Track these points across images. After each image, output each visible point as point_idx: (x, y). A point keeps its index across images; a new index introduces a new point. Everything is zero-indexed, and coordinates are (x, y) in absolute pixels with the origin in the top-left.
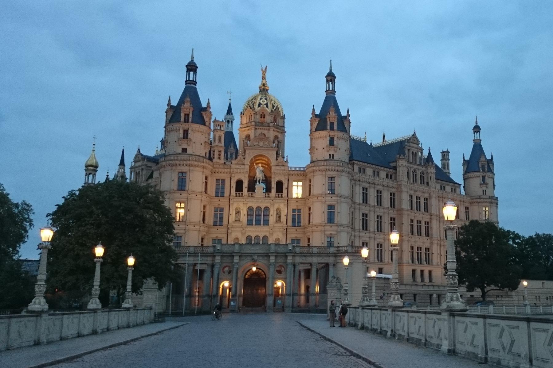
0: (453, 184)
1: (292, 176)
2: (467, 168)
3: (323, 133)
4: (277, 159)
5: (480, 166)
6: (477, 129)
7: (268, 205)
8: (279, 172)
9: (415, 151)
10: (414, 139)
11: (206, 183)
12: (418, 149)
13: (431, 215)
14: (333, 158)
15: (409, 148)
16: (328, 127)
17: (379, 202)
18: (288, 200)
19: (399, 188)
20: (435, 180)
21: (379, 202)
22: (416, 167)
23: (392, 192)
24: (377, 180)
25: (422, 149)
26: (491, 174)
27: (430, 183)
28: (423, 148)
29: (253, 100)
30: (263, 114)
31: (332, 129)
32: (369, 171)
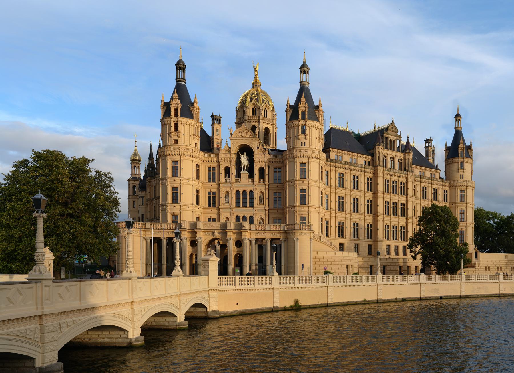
0: (431, 169)
1: (272, 164)
2: (448, 154)
3: (295, 123)
4: (258, 148)
9: (392, 138)
10: (392, 128)
11: (198, 171)
12: (396, 136)
13: (407, 198)
14: (305, 145)
15: (387, 135)
17: (356, 186)
21: (356, 186)
23: (368, 177)
25: (400, 137)
26: (469, 160)
27: (407, 168)
28: (402, 136)
29: (246, 96)
30: (254, 108)
31: (303, 118)
32: (347, 157)
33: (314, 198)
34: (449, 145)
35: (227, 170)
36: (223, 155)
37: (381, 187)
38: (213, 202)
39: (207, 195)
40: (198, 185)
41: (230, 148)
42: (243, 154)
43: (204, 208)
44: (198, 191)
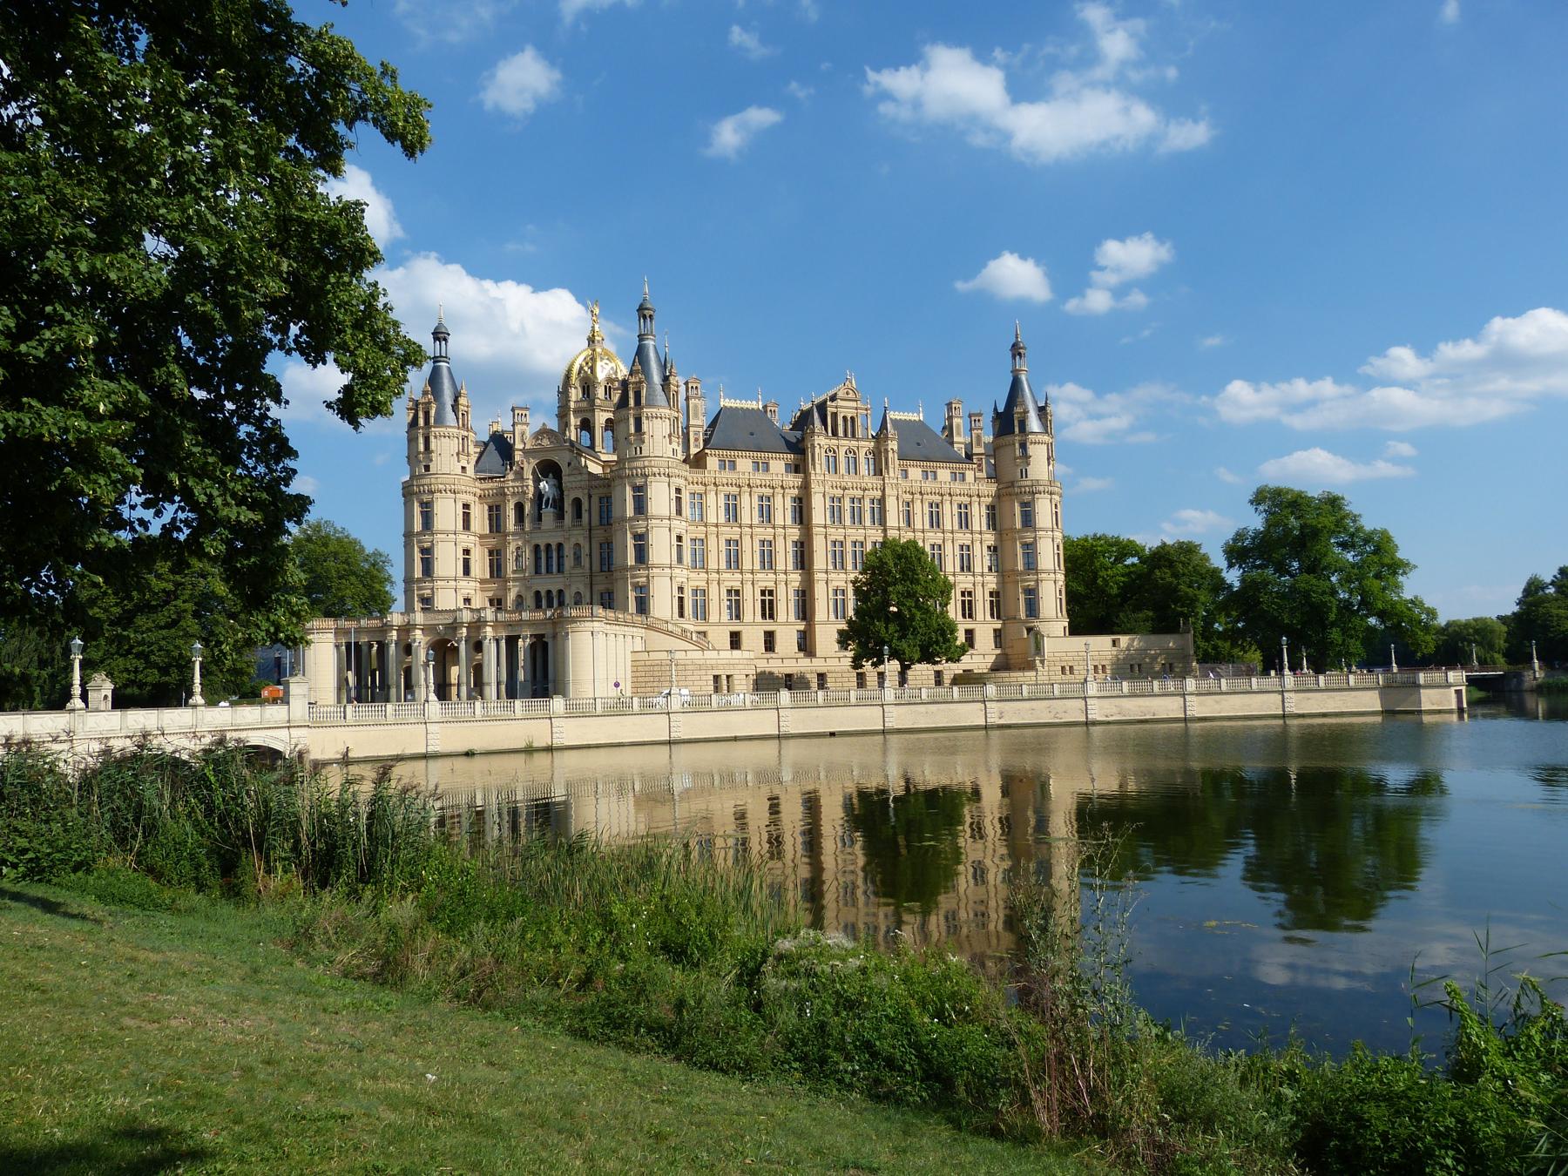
1: (596, 491)
4: (569, 464)
5: (1016, 423)
6: (1016, 350)
7: (560, 540)
8: (574, 485)
12: (856, 409)
15: (834, 410)
16: (632, 402)
18: (590, 530)
19: (806, 487)
20: (897, 462)
22: (854, 443)
24: (759, 477)
32: (744, 464)
33: (661, 548)
34: (1001, 409)
35: (519, 508)
36: (511, 484)
37: (819, 515)
38: (496, 568)
39: (487, 559)
40: (468, 540)
41: (522, 468)
42: (545, 476)
43: (482, 582)
44: (467, 552)
